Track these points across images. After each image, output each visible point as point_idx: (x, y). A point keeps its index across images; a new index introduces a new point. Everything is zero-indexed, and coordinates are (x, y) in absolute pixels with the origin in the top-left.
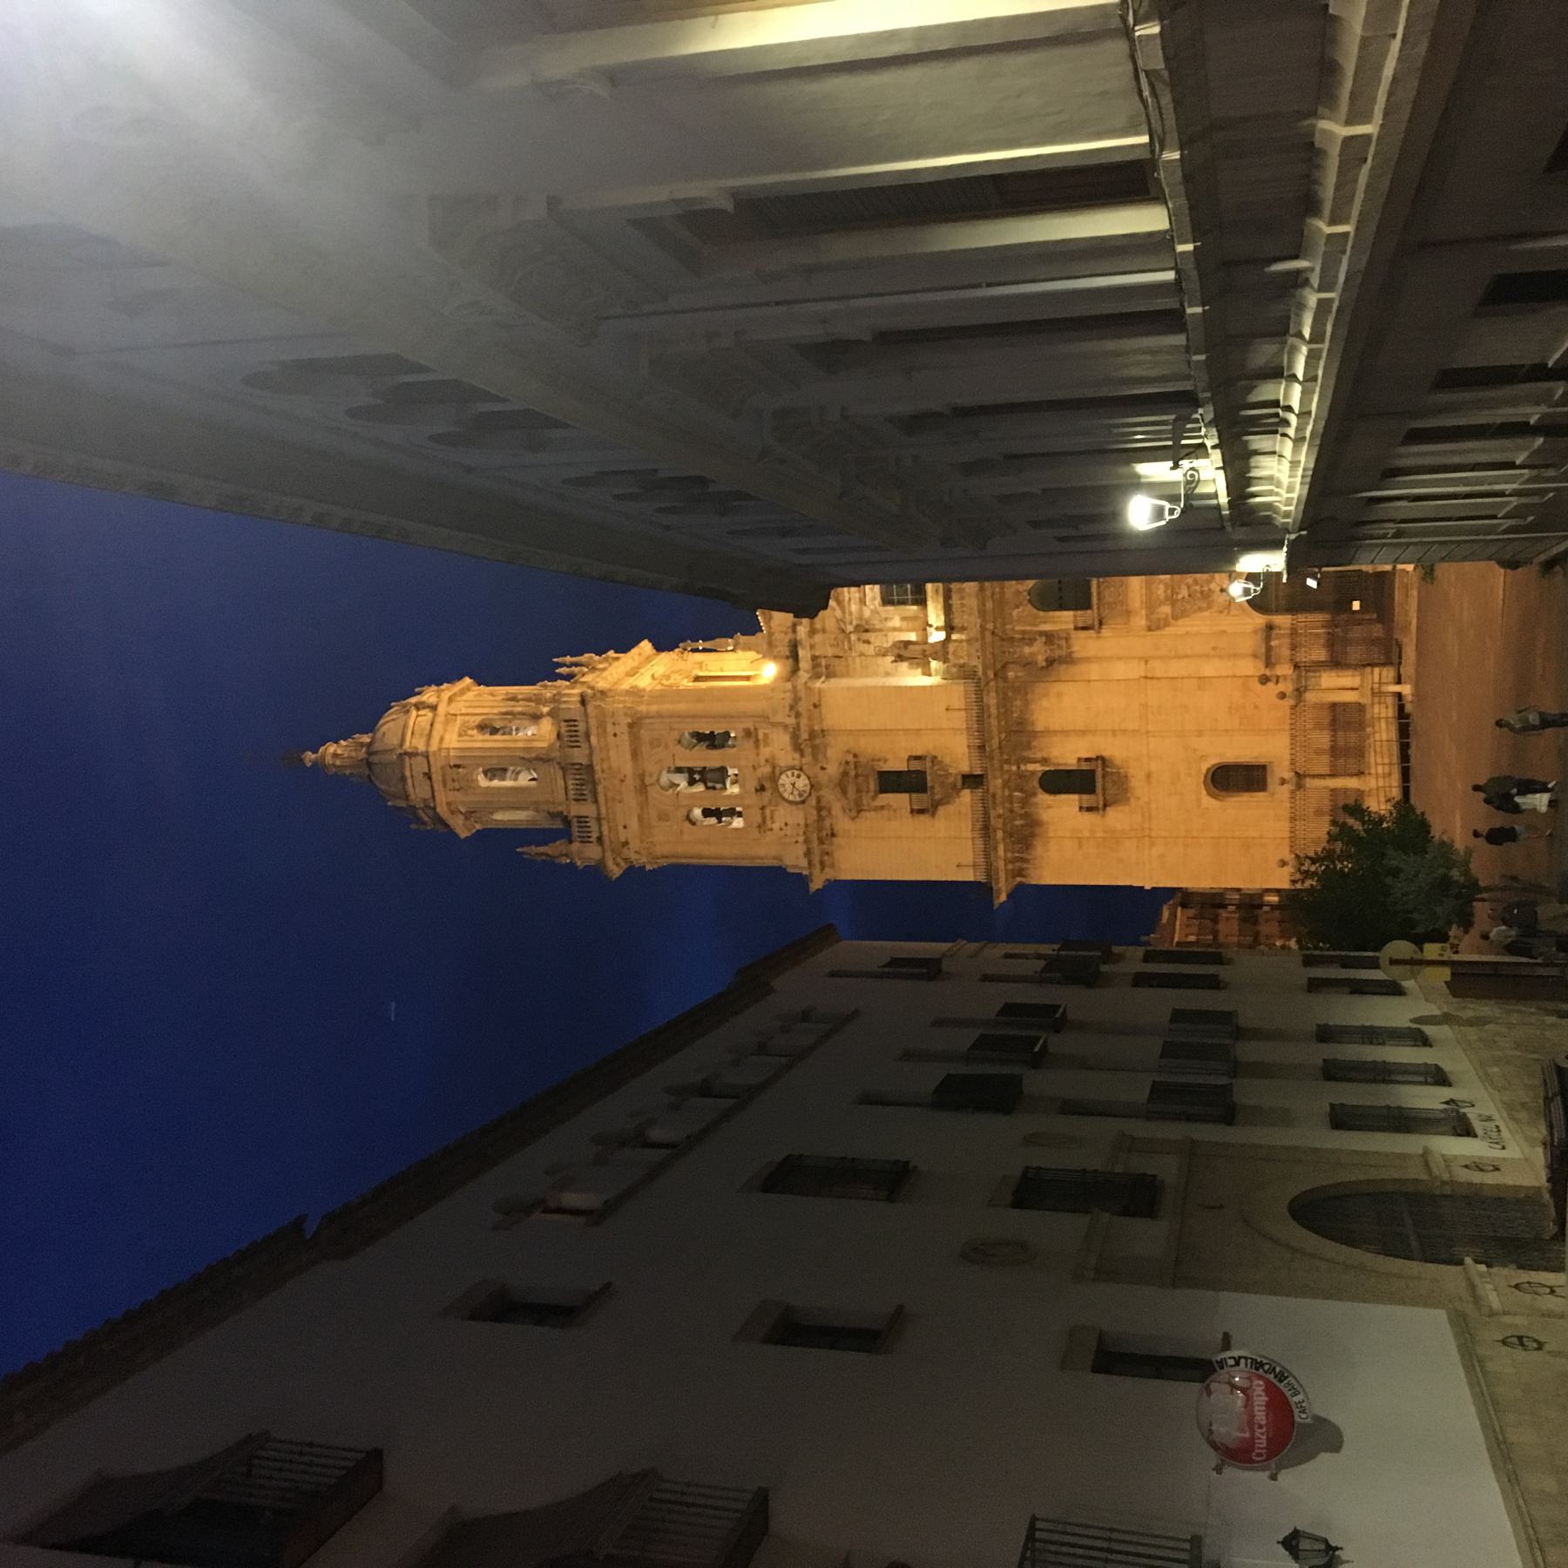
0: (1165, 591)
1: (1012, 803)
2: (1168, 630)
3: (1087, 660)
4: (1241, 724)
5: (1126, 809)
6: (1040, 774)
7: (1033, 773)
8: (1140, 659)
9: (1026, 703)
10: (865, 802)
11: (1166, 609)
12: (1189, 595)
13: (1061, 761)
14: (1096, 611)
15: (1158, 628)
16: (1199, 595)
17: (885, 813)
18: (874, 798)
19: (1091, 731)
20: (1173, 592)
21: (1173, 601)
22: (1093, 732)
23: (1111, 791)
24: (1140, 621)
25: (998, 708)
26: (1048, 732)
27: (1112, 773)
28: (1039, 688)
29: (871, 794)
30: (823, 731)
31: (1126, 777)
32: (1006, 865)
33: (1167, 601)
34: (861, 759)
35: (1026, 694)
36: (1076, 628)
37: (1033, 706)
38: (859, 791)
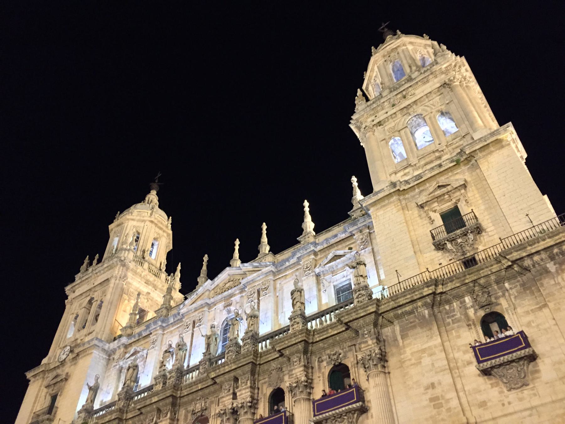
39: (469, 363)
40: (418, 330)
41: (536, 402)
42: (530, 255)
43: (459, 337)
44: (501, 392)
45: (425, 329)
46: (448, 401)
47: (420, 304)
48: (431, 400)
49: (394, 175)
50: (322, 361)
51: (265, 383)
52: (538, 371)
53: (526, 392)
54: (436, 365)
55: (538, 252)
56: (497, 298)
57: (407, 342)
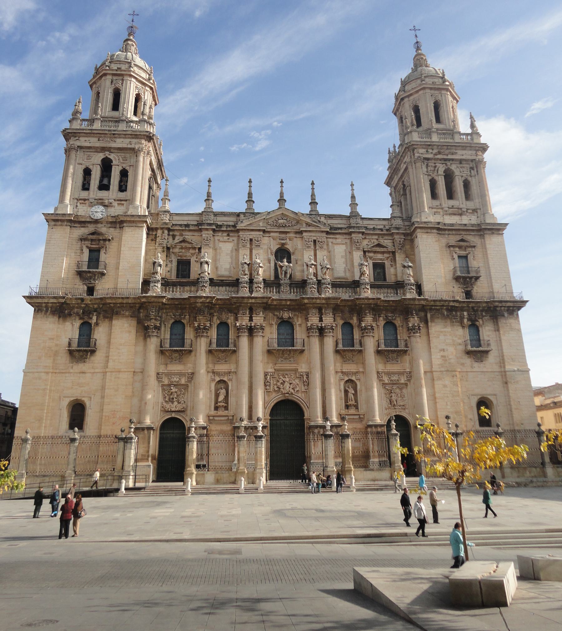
0: (175, 381)
1: (77, 308)
2: (156, 382)
3: (145, 345)
4: (106, 416)
5: (68, 362)
6: (90, 322)
7: (91, 318)
8: (143, 369)
9: (127, 317)
10: (86, 242)
11: (166, 382)
12: (172, 393)
13: (96, 332)
14: (169, 349)
15: (158, 378)
16: (171, 397)
17: (79, 251)
18: (87, 247)
19: (110, 345)
20: (175, 385)
21: (169, 385)
22: (109, 347)
23: (76, 354)
24: (162, 369)
25: (126, 303)
26: (111, 326)
27: (87, 355)
28: (134, 322)
29: (89, 246)
30: (123, 227)
31: (85, 362)
32: (45, 303)
33: (171, 382)
34: (107, 242)
35: (131, 317)
36: (161, 341)
37: (125, 319)
38: (92, 240)
39: (460, 344)
40: (440, 320)
41: (485, 370)
42: (501, 307)
43: (457, 330)
44: (471, 361)
45: (443, 321)
46: (450, 359)
47: (445, 308)
48: (442, 356)
49: (431, 209)
50: (381, 316)
51: (339, 316)
52: (487, 357)
53: (481, 365)
54: (447, 341)
55: (505, 307)
56: (479, 318)
57: (433, 324)
